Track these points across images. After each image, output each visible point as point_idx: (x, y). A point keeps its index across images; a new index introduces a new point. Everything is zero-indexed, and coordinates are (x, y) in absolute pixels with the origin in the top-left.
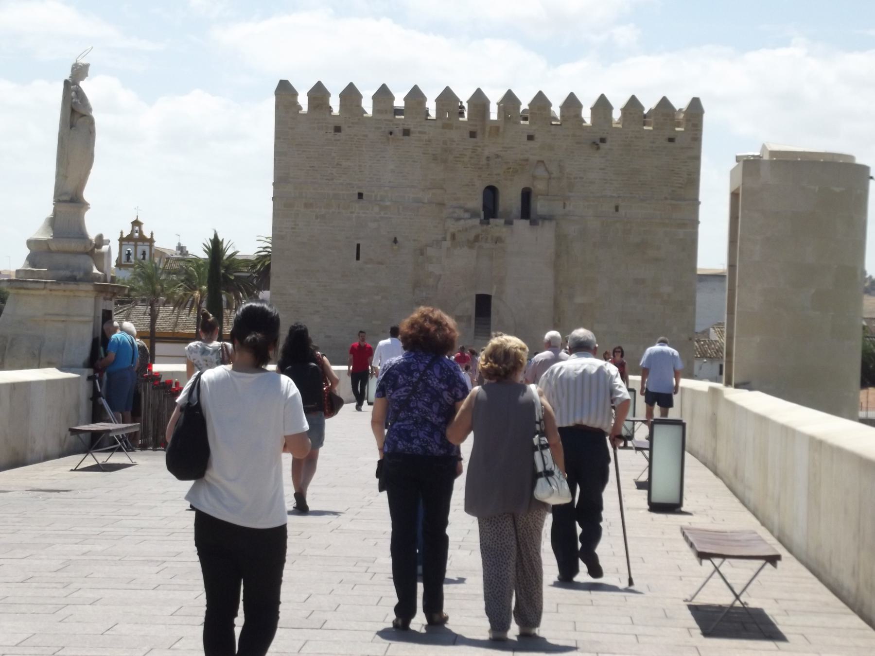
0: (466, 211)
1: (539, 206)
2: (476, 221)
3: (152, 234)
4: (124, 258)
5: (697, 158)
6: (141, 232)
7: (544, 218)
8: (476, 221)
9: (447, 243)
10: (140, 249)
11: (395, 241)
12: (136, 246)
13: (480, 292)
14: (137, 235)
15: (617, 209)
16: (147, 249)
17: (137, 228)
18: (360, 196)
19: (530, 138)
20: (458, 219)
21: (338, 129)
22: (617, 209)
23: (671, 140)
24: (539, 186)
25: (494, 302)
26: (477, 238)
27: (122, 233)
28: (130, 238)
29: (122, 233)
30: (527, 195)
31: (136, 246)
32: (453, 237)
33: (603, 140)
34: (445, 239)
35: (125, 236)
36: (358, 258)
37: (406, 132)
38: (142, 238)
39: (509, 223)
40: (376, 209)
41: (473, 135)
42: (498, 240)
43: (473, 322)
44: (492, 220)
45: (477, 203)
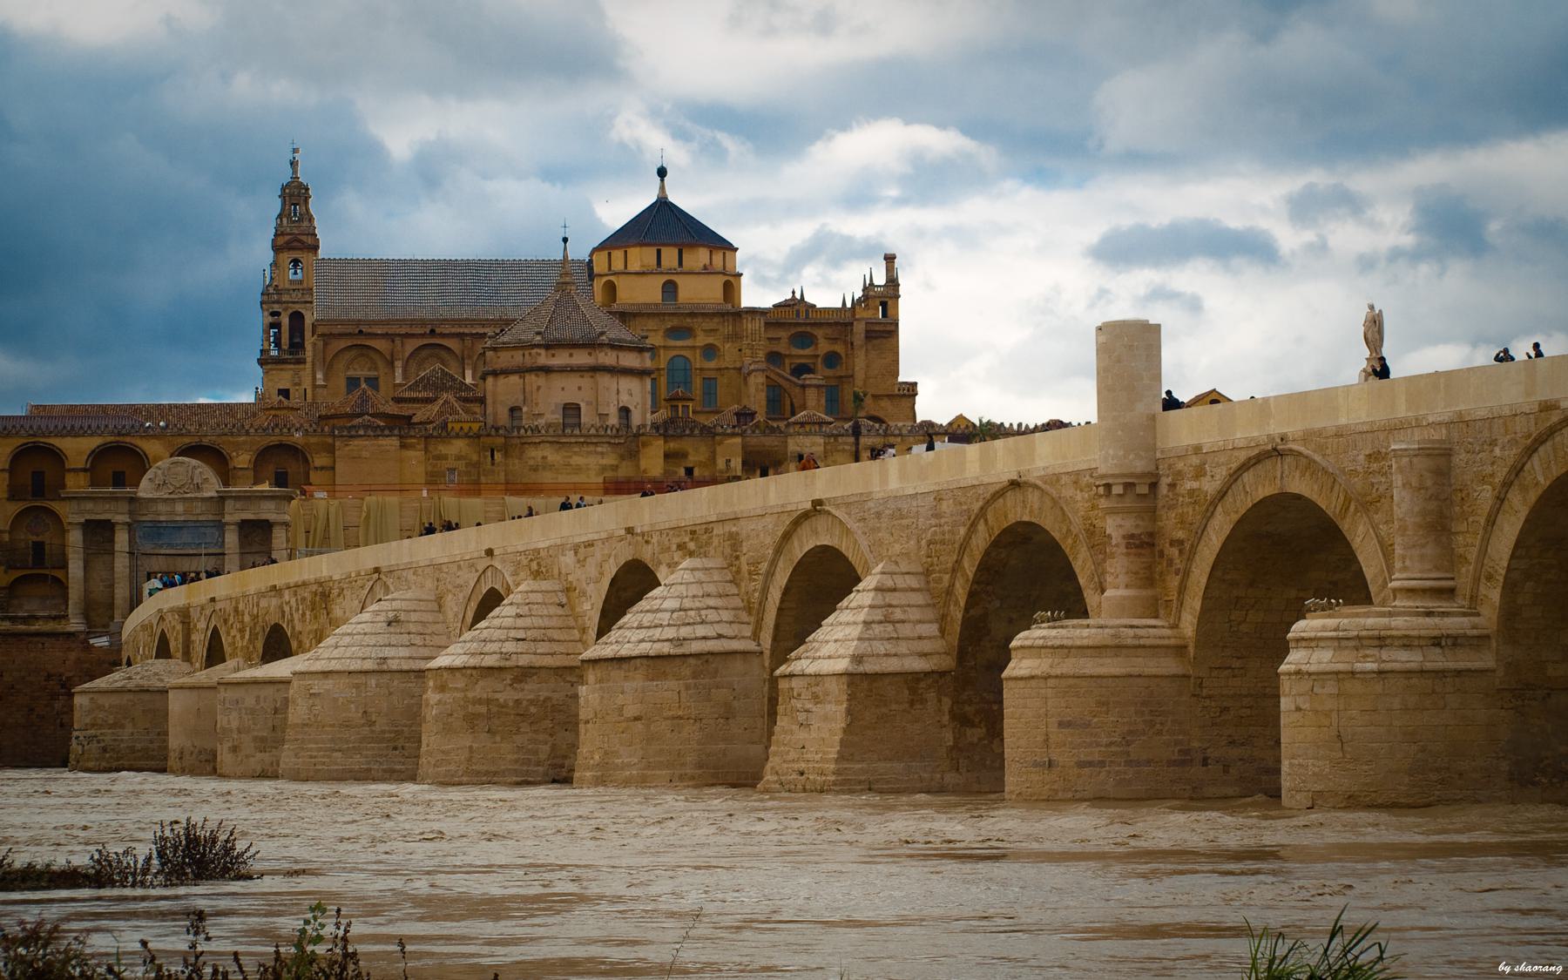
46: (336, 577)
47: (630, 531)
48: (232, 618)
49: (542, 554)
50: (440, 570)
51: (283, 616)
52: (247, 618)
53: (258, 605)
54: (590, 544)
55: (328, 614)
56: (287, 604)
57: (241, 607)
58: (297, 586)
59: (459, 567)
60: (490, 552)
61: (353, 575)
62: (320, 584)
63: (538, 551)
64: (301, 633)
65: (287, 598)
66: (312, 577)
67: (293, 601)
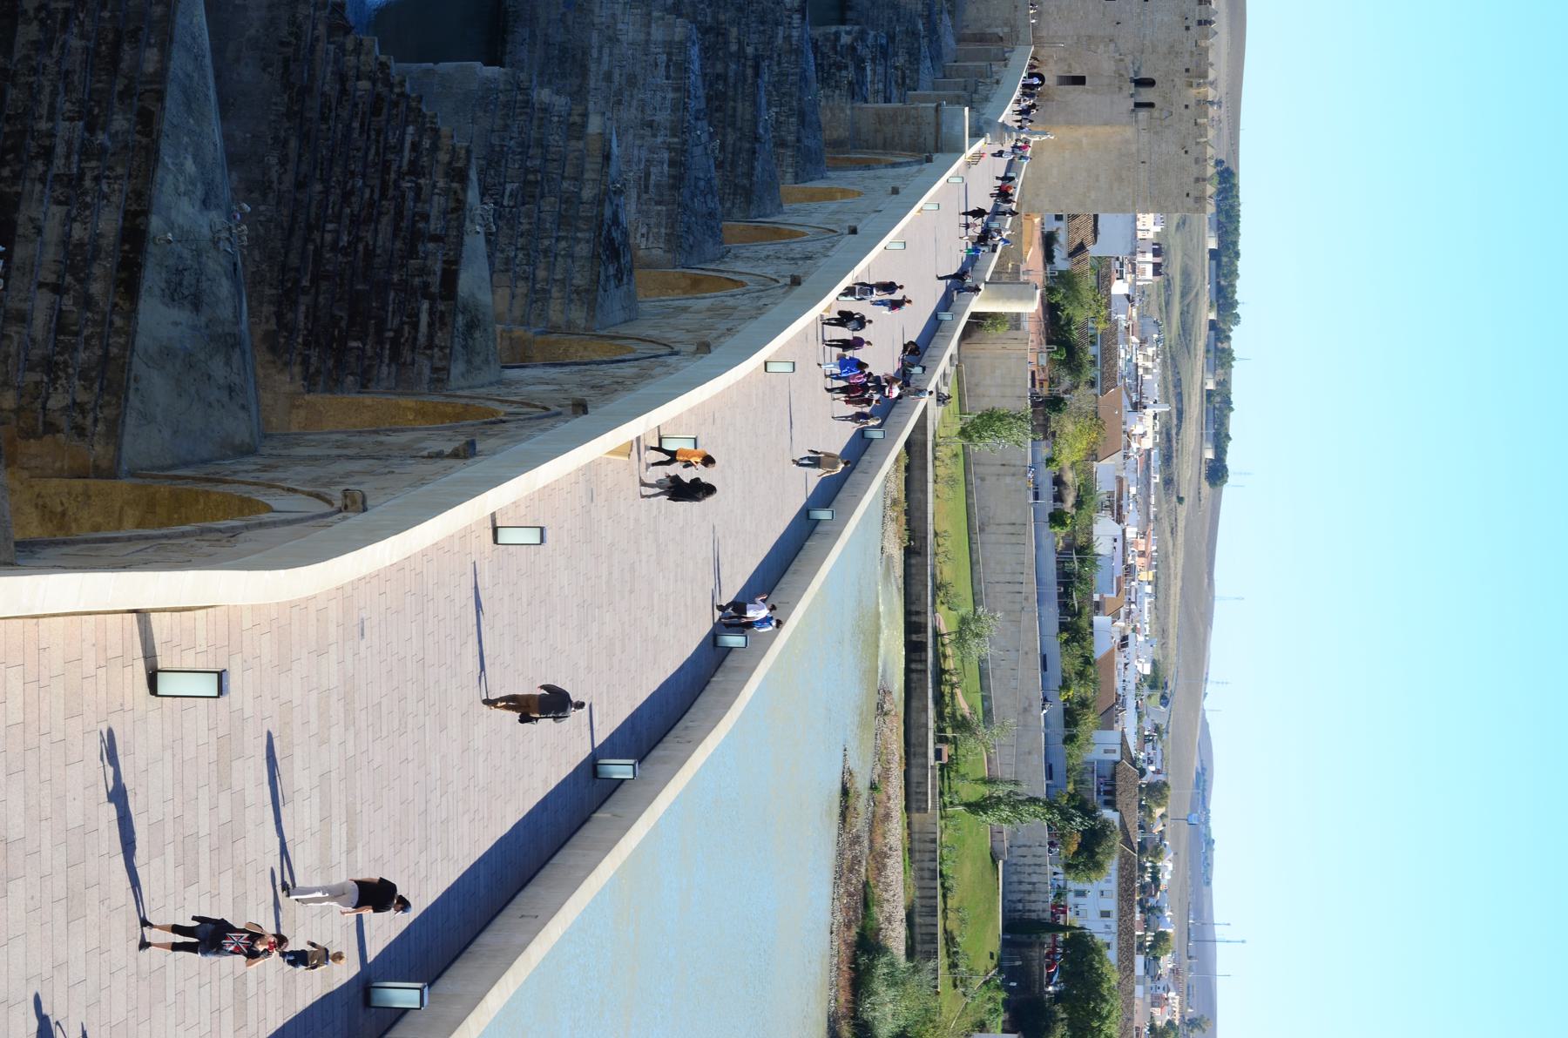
0: (1139, 68)
1: (1143, 114)
9: (1118, 57)
11: (1118, 23)
19: (1187, 107)
20: (1133, 64)
23: (1188, 195)
24: (1156, 112)
30: (1151, 105)
32: (1122, 60)
33: (1186, 152)
37: (1187, 28)
40: (1138, 11)
42: (1120, 88)
43: (1068, 75)
45: (1144, 74)
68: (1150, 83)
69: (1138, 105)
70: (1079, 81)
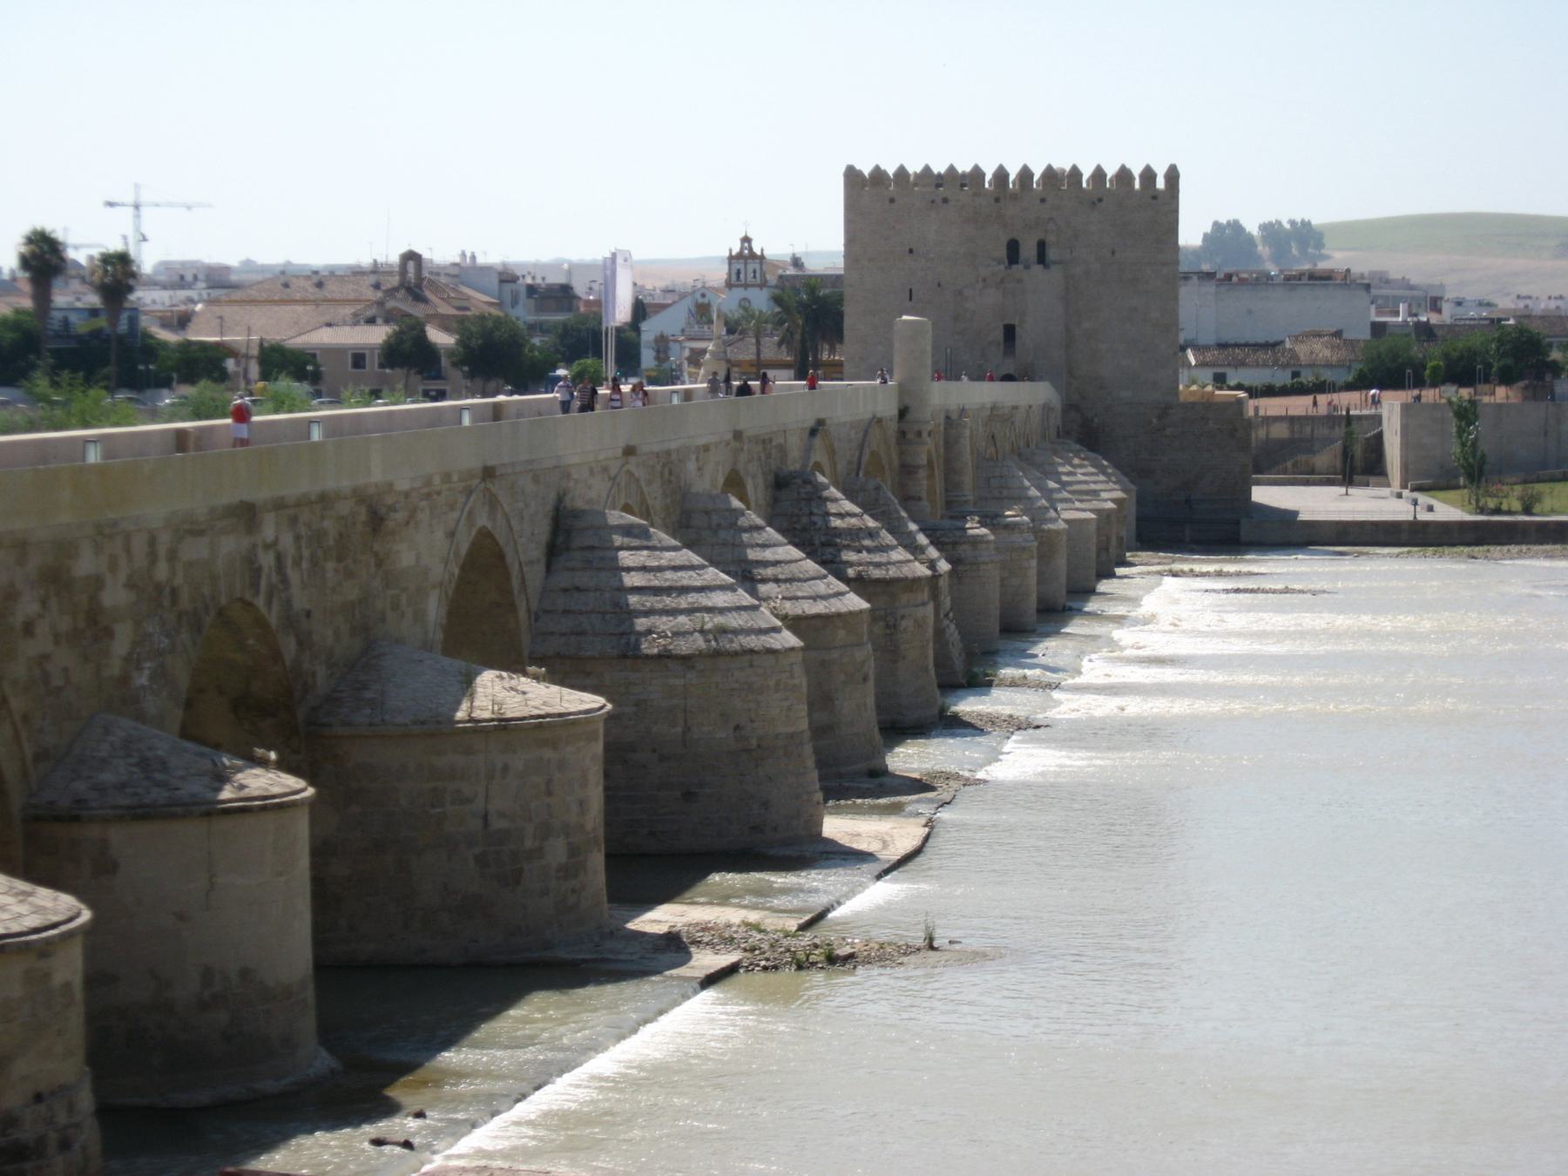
0: (994, 260)
1: (1052, 254)
2: (1002, 267)
3: (762, 250)
4: (734, 277)
5: (1176, 211)
6: (751, 249)
7: (1055, 263)
8: (1002, 267)
9: (980, 285)
10: (750, 267)
11: (939, 285)
12: (746, 264)
13: (1006, 322)
14: (746, 252)
15: (1113, 253)
16: (757, 267)
17: (746, 245)
18: (911, 251)
21: (892, 201)
22: (1113, 253)
23: (1154, 198)
24: (1051, 238)
25: (1018, 329)
26: (1002, 281)
27: (731, 250)
28: (740, 256)
29: (731, 250)
30: (1042, 246)
31: (746, 264)
32: (984, 280)
33: (1100, 200)
34: (977, 282)
35: (734, 253)
36: (911, 299)
38: (753, 255)
39: (1027, 267)
41: (997, 200)
43: (1002, 346)
44: (1014, 267)
45: (1002, 252)
46: (403, 485)
47: (738, 435)
48: (28, 606)
49: (674, 457)
50: (568, 476)
51: (255, 586)
52: (115, 596)
53: (172, 556)
54: (706, 448)
55: (379, 564)
56: (267, 547)
57: (85, 564)
58: (298, 504)
59: (592, 471)
60: (629, 451)
61: (437, 480)
62: (360, 496)
63: (668, 453)
64: (308, 614)
65: (268, 531)
66: (346, 484)
67: (287, 542)
68: (1013, 249)
69: (1042, 258)
70: (1010, 332)
